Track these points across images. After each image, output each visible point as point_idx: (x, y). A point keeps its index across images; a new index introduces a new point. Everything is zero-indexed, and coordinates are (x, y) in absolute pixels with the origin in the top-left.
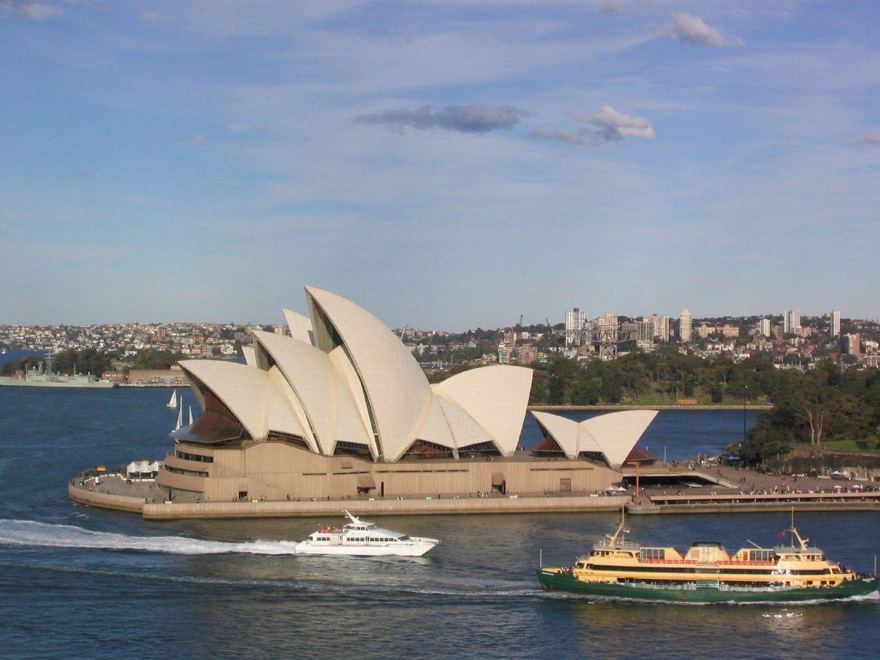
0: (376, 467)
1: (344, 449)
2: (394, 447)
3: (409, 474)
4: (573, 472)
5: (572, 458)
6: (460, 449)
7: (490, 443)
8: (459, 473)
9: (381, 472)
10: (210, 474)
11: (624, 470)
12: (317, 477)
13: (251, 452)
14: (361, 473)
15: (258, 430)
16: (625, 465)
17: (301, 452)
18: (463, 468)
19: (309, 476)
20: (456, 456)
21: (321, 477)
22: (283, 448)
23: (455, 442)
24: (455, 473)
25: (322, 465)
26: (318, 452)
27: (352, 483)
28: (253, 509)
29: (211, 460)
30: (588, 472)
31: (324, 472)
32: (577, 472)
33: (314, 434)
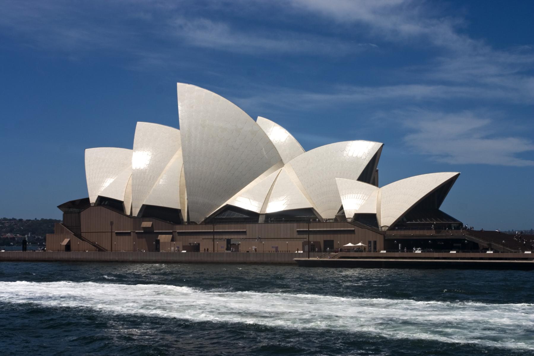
1: (148, 211)
5: (349, 220)
7: (310, 211)
13: (84, 214)
20: (261, 219)
26: (128, 213)
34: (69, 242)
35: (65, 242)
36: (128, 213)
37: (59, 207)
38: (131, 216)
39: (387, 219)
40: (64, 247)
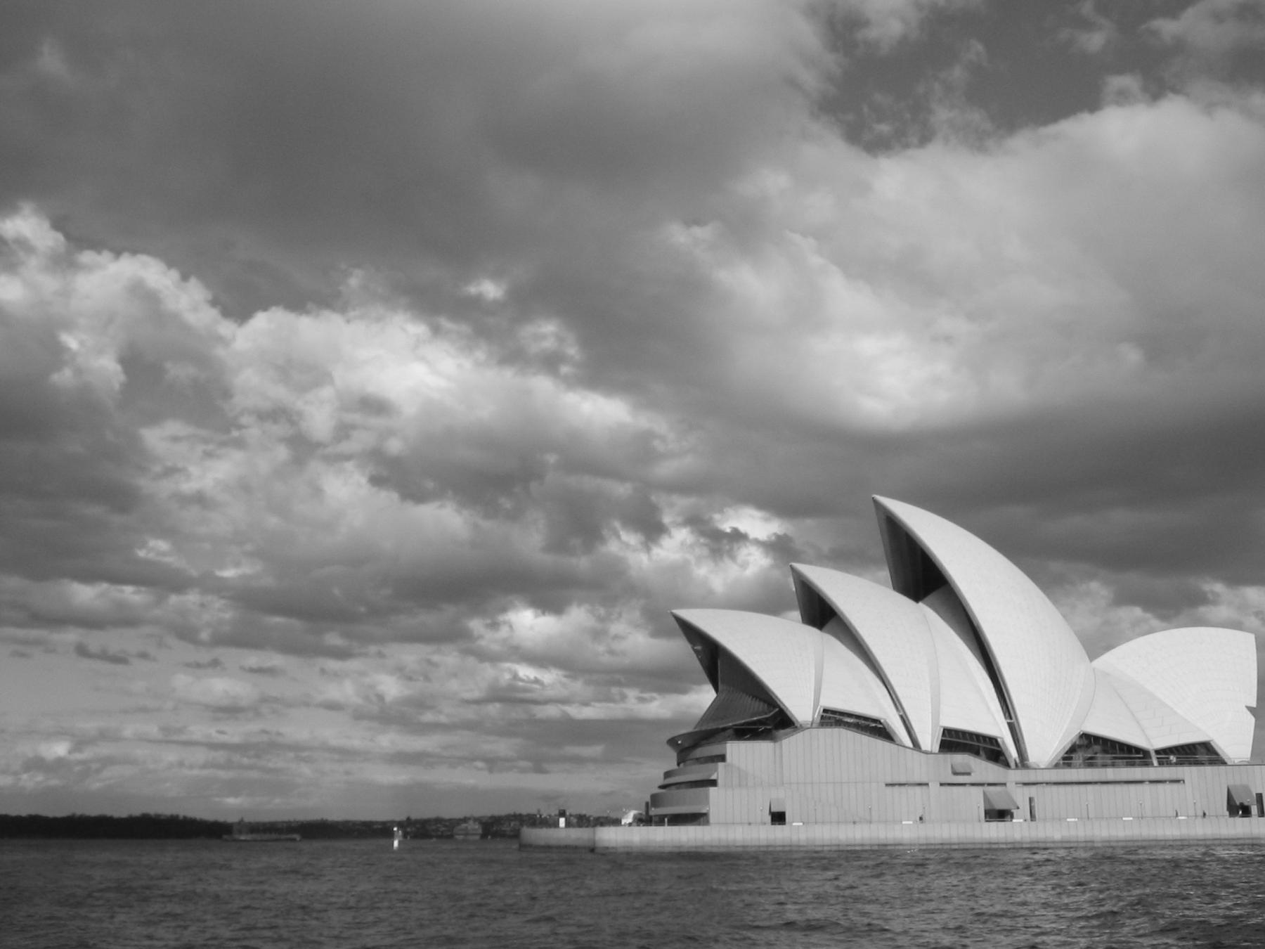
0: (1014, 775)
2: (1045, 741)
3: (1076, 788)
6: (1158, 752)
8: (1168, 786)
9: (1025, 784)
10: (719, 782)
12: (911, 790)
13: (790, 743)
14: (990, 784)
17: (880, 744)
18: (1174, 777)
21: (918, 789)
23: (1148, 740)
24: (1160, 786)
25: (918, 767)
26: (909, 744)
27: (975, 800)
28: (795, 838)
29: (722, 758)
31: (924, 780)
33: (901, 717)
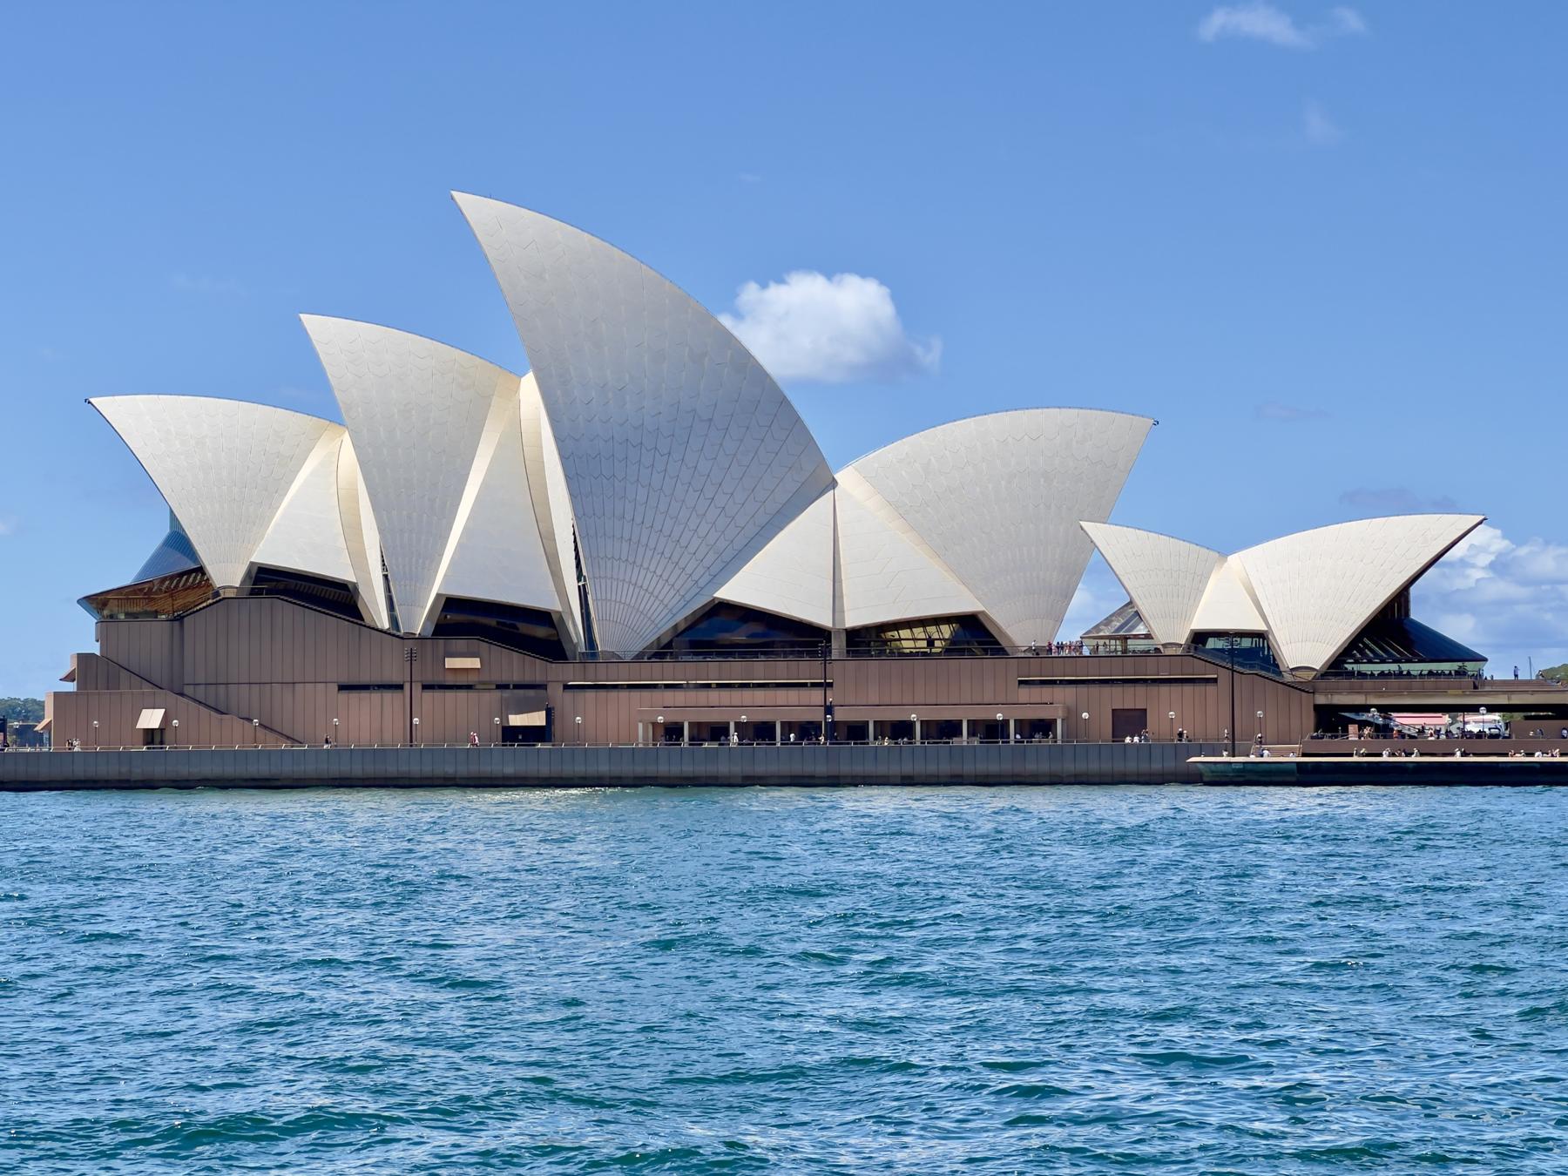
1: (464, 618)
4: (1154, 689)
11: (1322, 684)
15: (227, 574)
16: (1336, 666)
19: (354, 695)
20: (838, 645)
22: (287, 613)
26: (386, 625)
30: (1199, 688)
31: (396, 680)
32: (1164, 689)
34: (166, 719)
35: (151, 718)
36: (385, 624)
37: (97, 603)
38: (394, 632)
39: (1306, 645)
40: (141, 737)
